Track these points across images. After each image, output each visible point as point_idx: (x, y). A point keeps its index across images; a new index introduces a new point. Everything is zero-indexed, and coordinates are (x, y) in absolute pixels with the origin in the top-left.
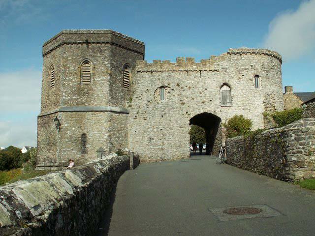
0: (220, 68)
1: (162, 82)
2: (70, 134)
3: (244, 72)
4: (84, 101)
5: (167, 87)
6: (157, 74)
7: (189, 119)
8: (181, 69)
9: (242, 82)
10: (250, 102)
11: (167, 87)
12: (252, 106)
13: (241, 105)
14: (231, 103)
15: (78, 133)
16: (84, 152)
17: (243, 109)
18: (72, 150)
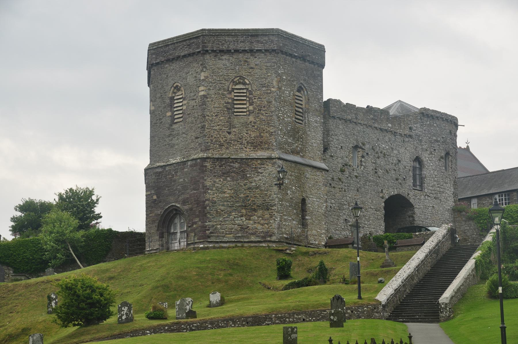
0: (413, 133)
1: (357, 140)
2: (291, 196)
3: (436, 145)
4: (299, 149)
5: (361, 148)
6: (351, 125)
7: (384, 200)
8: (376, 125)
9: (434, 159)
10: (441, 190)
11: (361, 148)
12: (443, 194)
13: (433, 192)
14: (421, 186)
15: (298, 196)
16: (304, 224)
17: (435, 198)
18: (293, 220)
